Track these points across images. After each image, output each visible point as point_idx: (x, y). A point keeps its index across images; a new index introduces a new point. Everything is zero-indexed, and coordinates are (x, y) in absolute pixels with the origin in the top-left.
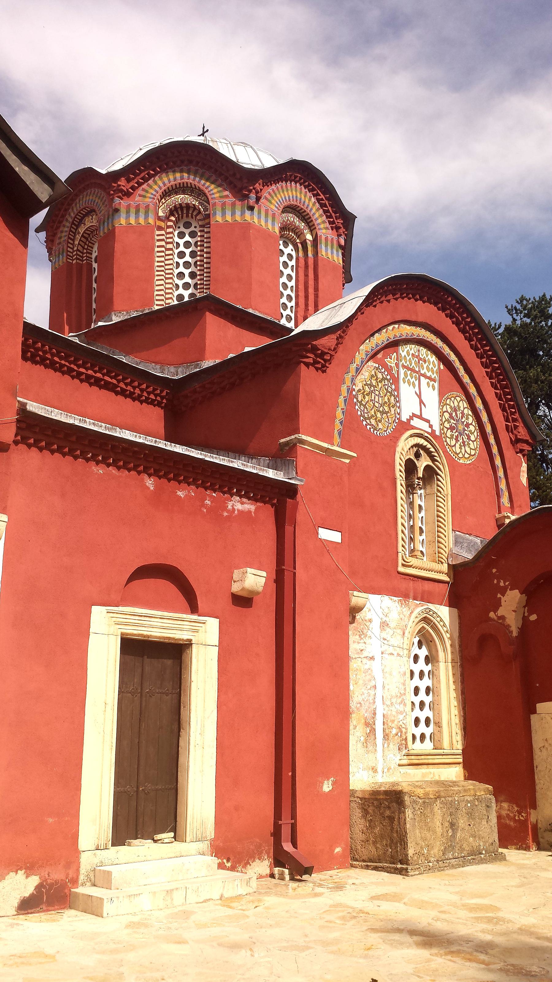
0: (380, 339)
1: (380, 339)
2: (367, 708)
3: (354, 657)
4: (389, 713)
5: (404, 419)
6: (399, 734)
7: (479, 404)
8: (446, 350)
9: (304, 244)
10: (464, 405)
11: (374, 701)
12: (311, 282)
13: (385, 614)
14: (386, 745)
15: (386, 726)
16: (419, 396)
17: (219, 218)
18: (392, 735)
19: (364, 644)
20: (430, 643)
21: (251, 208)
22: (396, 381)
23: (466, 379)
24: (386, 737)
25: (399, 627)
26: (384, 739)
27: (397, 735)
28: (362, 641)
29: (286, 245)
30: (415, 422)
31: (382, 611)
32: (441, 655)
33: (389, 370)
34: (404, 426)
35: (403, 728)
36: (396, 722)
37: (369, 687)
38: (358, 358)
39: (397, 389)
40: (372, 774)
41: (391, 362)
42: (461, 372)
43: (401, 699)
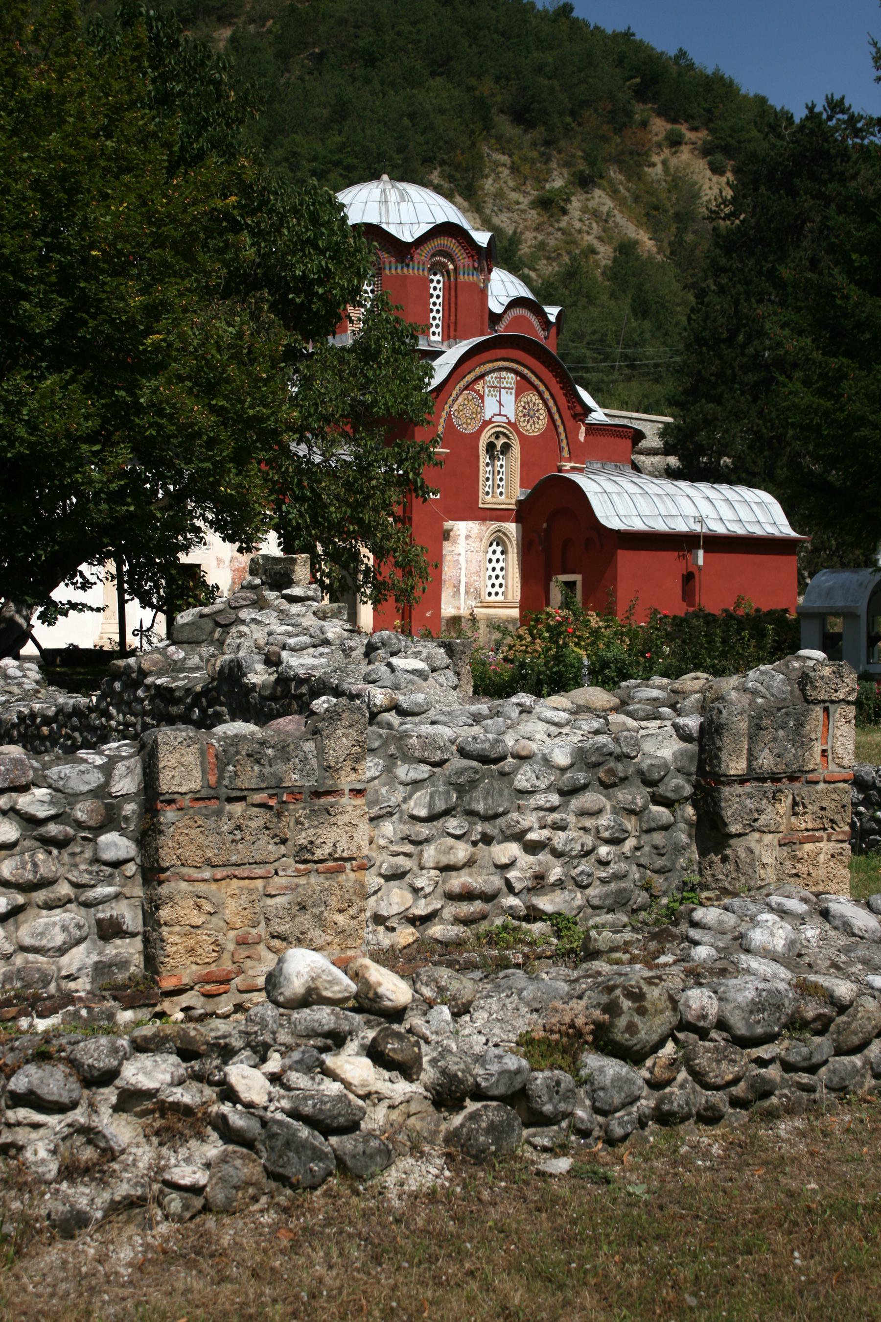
0: (470, 377)
1: (470, 377)
5: (487, 419)
7: (547, 395)
8: (521, 368)
9: (448, 272)
10: (535, 398)
12: (453, 299)
16: (500, 402)
17: (387, 272)
21: (408, 266)
22: (482, 397)
23: (537, 382)
24: (467, 593)
29: (435, 274)
30: (496, 419)
32: (510, 550)
33: (477, 392)
34: (486, 423)
38: (454, 393)
39: (483, 402)
41: (478, 387)
42: (533, 378)
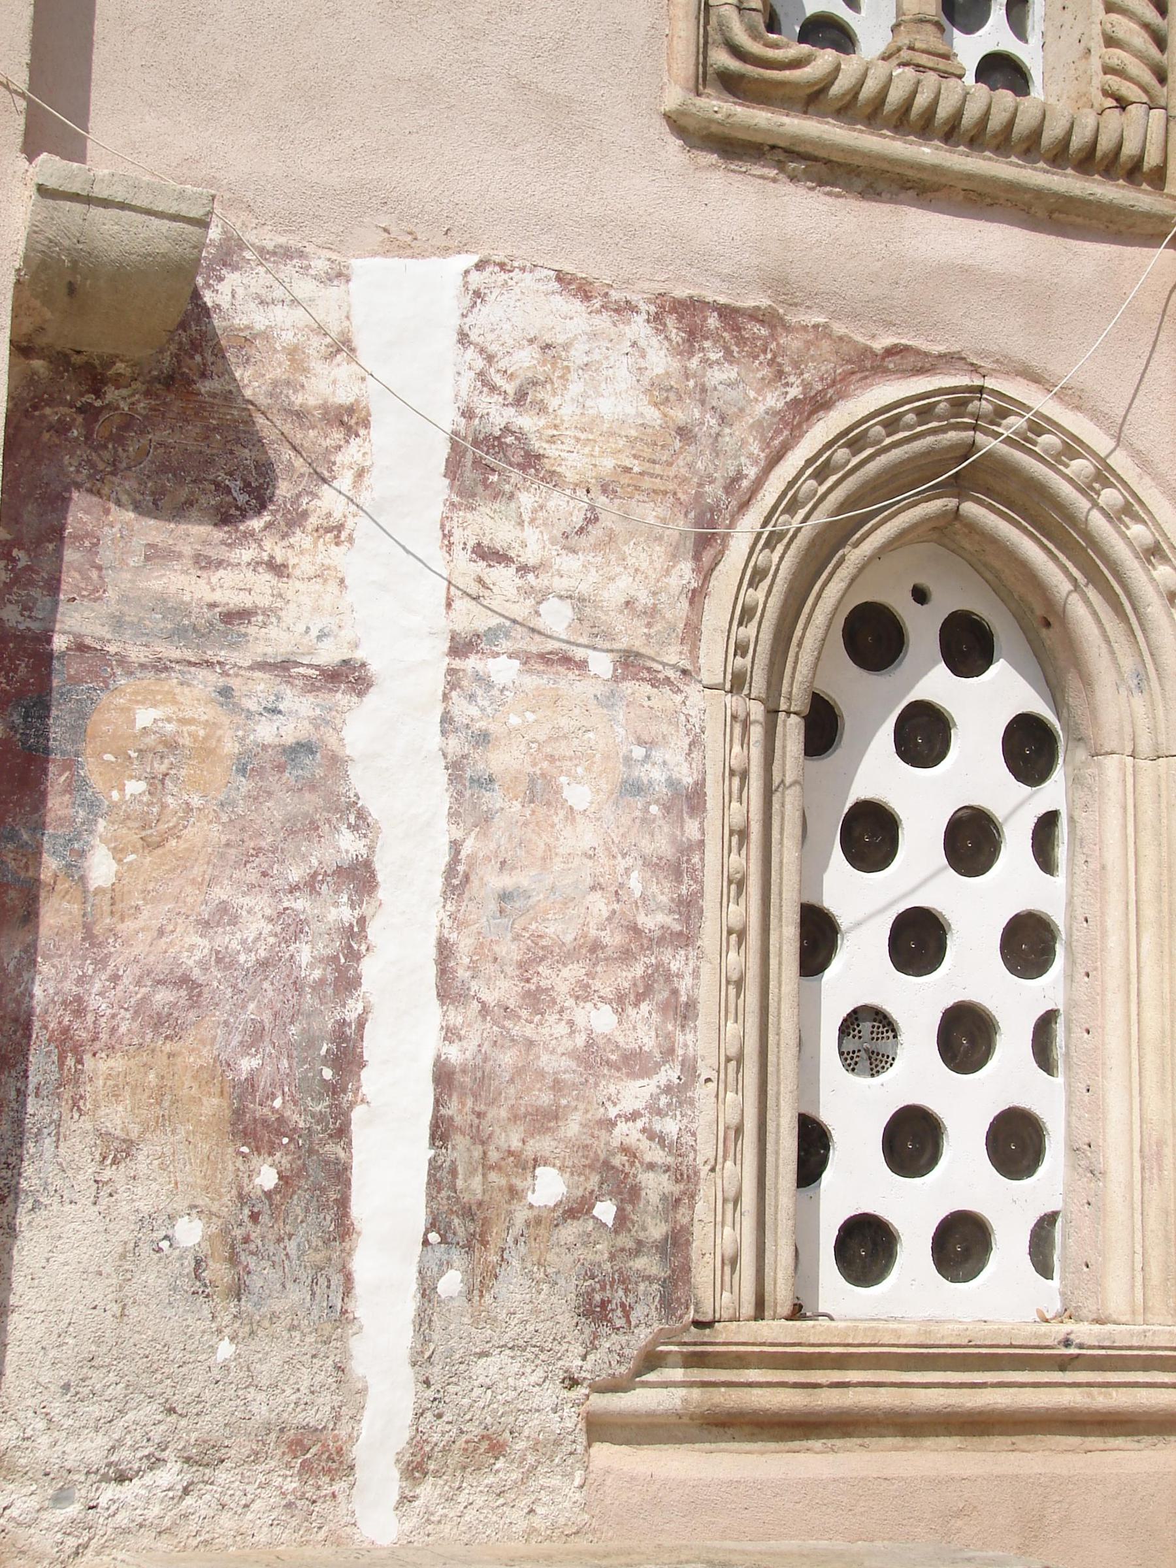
2: (267, 1017)
3: (137, 654)
4: (508, 1058)
6: (605, 1211)
11: (341, 971)
13: (510, 388)
14: (451, 1283)
15: (460, 1149)
18: (521, 1216)
19: (266, 578)
20: (1044, 632)
25: (647, 483)
26: (434, 1237)
27: (576, 1209)
28: (247, 554)
31: (480, 364)
35: (651, 1166)
36: (572, 1128)
37: (296, 874)
40: (291, 1485)
43: (639, 970)
